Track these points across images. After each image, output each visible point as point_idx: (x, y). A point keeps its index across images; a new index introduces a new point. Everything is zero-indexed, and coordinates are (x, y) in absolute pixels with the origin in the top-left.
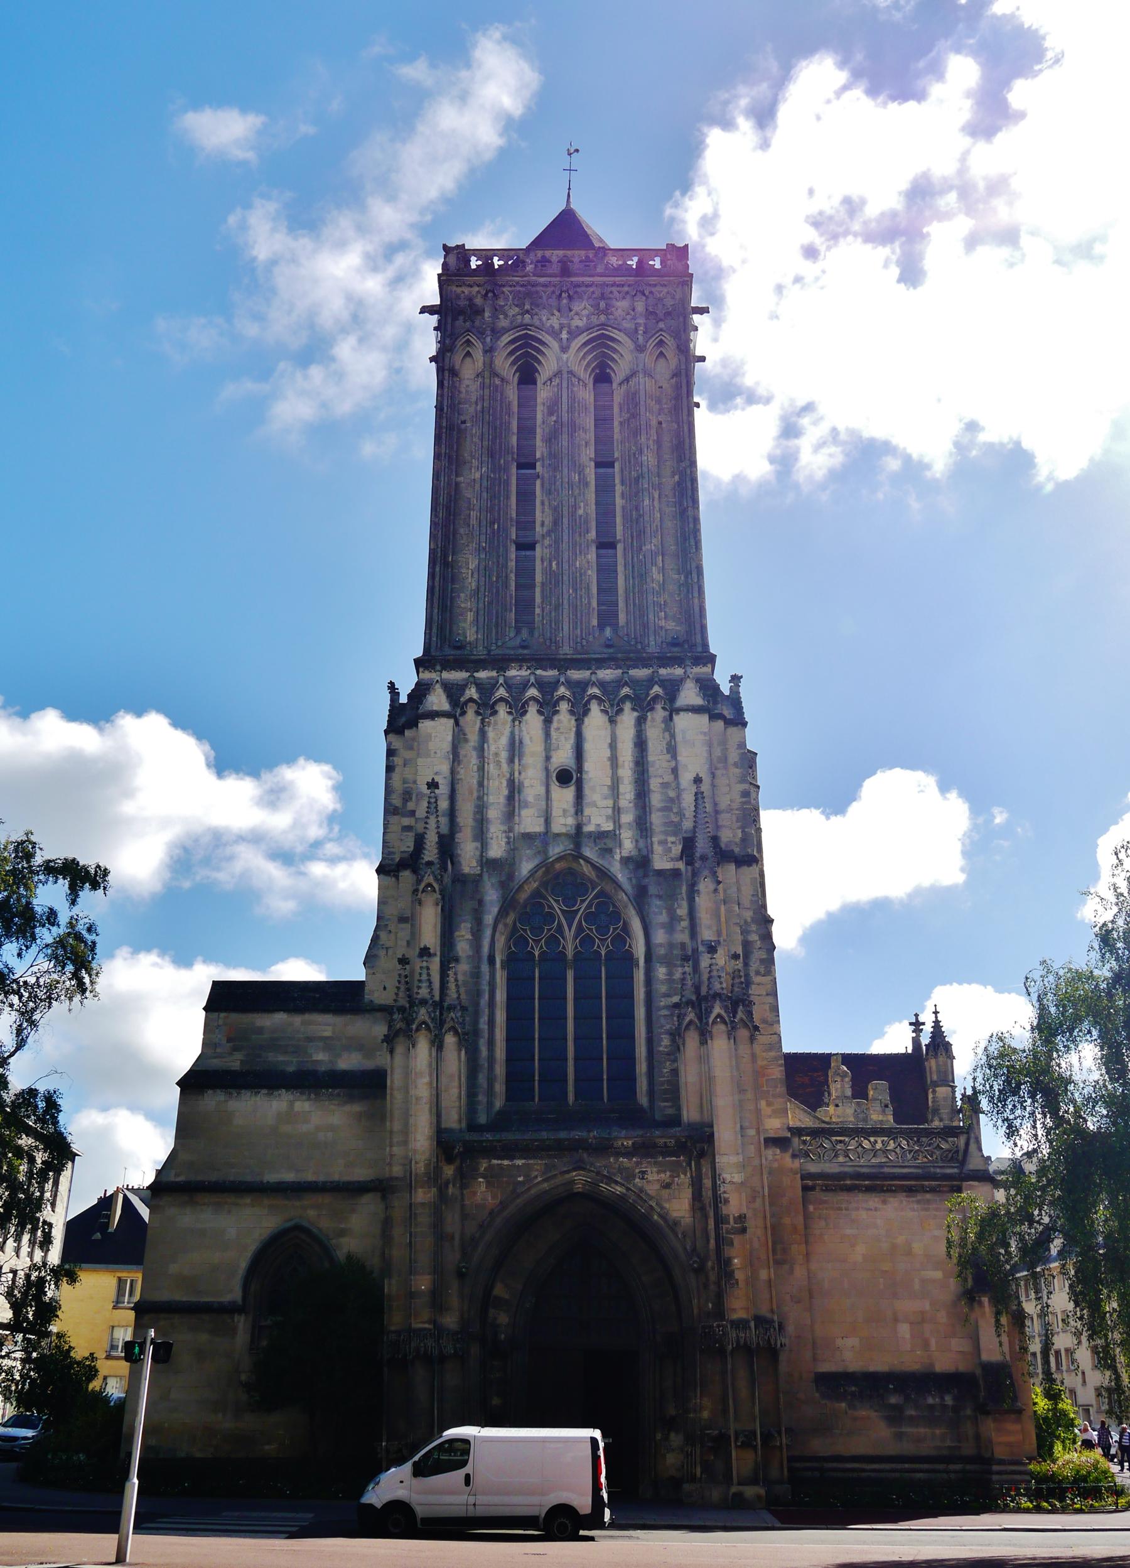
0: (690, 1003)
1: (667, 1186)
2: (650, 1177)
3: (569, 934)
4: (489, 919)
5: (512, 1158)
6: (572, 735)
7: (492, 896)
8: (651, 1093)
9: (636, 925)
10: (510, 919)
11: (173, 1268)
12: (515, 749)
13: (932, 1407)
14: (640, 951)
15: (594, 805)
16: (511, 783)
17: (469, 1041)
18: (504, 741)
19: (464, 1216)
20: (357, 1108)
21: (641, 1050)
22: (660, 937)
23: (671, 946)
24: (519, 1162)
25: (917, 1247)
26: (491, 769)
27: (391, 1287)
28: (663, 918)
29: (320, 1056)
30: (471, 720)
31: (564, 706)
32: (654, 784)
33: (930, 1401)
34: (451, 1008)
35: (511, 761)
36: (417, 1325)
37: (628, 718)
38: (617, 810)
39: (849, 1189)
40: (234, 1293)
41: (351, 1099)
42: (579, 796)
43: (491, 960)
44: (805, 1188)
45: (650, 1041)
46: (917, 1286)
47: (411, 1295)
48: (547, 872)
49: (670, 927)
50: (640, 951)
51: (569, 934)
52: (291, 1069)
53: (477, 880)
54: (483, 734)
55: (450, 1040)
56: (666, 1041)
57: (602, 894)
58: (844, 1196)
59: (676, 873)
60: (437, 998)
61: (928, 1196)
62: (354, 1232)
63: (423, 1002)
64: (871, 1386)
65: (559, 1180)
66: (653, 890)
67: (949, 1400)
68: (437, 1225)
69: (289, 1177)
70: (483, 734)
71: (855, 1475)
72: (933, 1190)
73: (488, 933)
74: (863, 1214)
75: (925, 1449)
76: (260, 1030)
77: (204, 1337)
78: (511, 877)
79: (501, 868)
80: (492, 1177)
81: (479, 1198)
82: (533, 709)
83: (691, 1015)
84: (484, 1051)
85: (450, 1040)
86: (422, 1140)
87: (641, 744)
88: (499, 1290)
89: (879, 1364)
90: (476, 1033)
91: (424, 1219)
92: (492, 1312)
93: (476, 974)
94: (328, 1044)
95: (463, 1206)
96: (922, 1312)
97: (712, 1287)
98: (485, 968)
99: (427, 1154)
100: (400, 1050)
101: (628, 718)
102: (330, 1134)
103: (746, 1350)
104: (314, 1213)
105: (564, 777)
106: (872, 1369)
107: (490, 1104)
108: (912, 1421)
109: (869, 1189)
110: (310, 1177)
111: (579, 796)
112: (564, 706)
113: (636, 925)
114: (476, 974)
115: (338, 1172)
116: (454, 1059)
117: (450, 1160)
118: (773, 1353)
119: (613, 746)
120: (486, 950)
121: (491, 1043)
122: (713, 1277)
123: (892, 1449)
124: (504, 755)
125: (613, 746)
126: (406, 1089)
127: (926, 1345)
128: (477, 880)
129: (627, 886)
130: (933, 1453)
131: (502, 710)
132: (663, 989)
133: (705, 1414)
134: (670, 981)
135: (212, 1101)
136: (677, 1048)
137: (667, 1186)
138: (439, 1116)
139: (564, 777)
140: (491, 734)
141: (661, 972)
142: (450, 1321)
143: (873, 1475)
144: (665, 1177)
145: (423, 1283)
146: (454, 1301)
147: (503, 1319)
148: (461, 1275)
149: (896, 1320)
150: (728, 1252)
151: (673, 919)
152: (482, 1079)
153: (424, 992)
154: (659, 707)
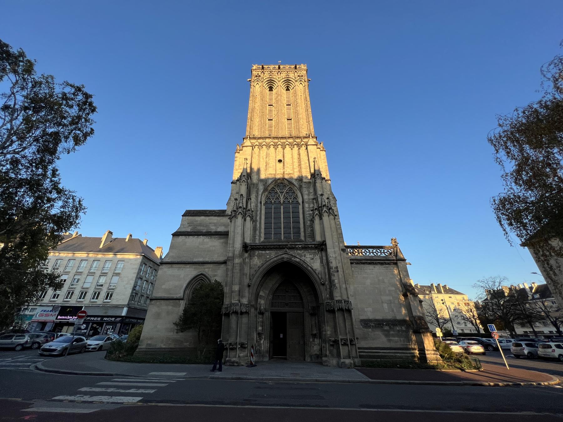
0: (316, 209)
1: (312, 259)
2: (306, 256)
3: (282, 197)
4: (260, 193)
5: (265, 251)
6: (282, 153)
7: (261, 188)
8: (305, 236)
9: (299, 195)
10: (266, 193)
11: (163, 287)
12: (267, 155)
13: (398, 330)
14: (300, 201)
15: (288, 167)
16: (266, 163)
17: (253, 220)
18: (265, 154)
19: (250, 268)
20: (222, 241)
21: (302, 226)
22: (306, 197)
23: (309, 199)
24: (268, 252)
25: (386, 281)
26: (261, 160)
27: (226, 290)
28: (307, 192)
29: (213, 228)
30: (256, 149)
31: (280, 146)
32: (302, 163)
33: (398, 329)
34: (249, 210)
35: (266, 158)
36: (233, 302)
37: (296, 148)
38: (293, 168)
39: (364, 263)
40: (181, 295)
41: (220, 238)
42: (284, 165)
43: (261, 203)
44: (351, 263)
45: (304, 223)
46: (387, 292)
47: (232, 292)
48: (275, 183)
49: (309, 195)
50: (300, 201)
51: (282, 197)
52: (204, 231)
53: (257, 184)
54: (259, 152)
55: (248, 219)
56: (309, 222)
57: (290, 187)
58: (363, 265)
59: (310, 182)
60: (245, 207)
61: (387, 266)
62: (217, 275)
63: (240, 207)
64: (379, 324)
65: (280, 257)
66: (303, 186)
67: (404, 328)
68: (242, 270)
69: (201, 260)
70: (259, 152)
71: (377, 354)
72: (388, 264)
73: (260, 196)
74: (369, 271)
75: (398, 345)
76: (197, 221)
77: (170, 307)
78: (266, 183)
79: (265, 181)
80: (259, 256)
81: (255, 263)
82: (272, 147)
83: (317, 212)
84: (258, 226)
85: (248, 219)
86: (238, 246)
87: (299, 154)
88: (261, 293)
89: (379, 317)
90: (256, 221)
91: (237, 268)
92: (259, 300)
93: (257, 206)
94: (215, 225)
95: (250, 265)
96: (390, 300)
97: (328, 290)
98: (259, 204)
99: (240, 249)
100: (233, 221)
101: (296, 148)
102: (214, 248)
103: (341, 310)
104: (208, 270)
105: (280, 161)
106: (377, 318)
107: (260, 239)
108: (393, 336)
109: (370, 264)
110: (207, 260)
111: (284, 165)
112: (280, 146)
113: (299, 195)
114: (257, 206)
115: (216, 258)
116: (249, 224)
117: (247, 252)
118: (349, 311)
119: (292, 155)
120: (259, 201)
121: (260, 223)
122: (328, 287)
123: (388, 345)
124: (265, 157)
125: (292, 155)
126: (234, 232)
127: (393, 311)
128: (257, 184)
129: (297, 185)
130: (402, 346)
131: (264, 147)
132: (307, 209)
133: (329, 333)
134: (309, 208)
135: (181, 238)
136: (312, 221)
137: (312, 259)
138: (244, 239)
139: (280, 161)
140: (261, 152)
141: (307, 205)
142: (245, 301)
143: (383, 354)
144: (312, 256)
145: (236, 288)
146: (247, 294)
147: (262, 302)
148: (249, 286)
149: (382, 302)
150: (333, 278)
151: (309, 193)
152: (257, 232)
153: (241, 205)
154: (303, 146)
